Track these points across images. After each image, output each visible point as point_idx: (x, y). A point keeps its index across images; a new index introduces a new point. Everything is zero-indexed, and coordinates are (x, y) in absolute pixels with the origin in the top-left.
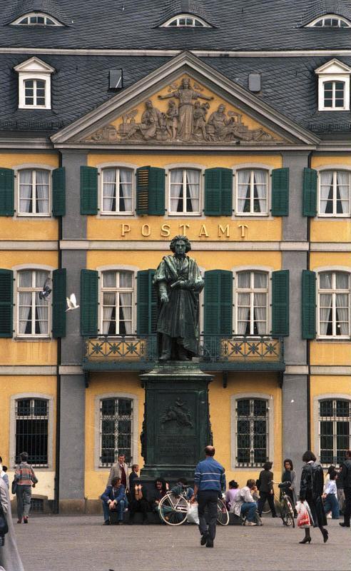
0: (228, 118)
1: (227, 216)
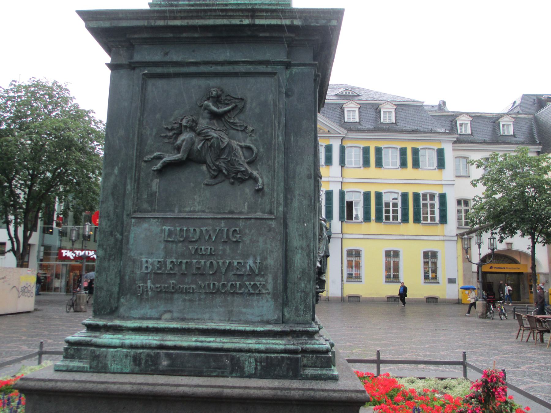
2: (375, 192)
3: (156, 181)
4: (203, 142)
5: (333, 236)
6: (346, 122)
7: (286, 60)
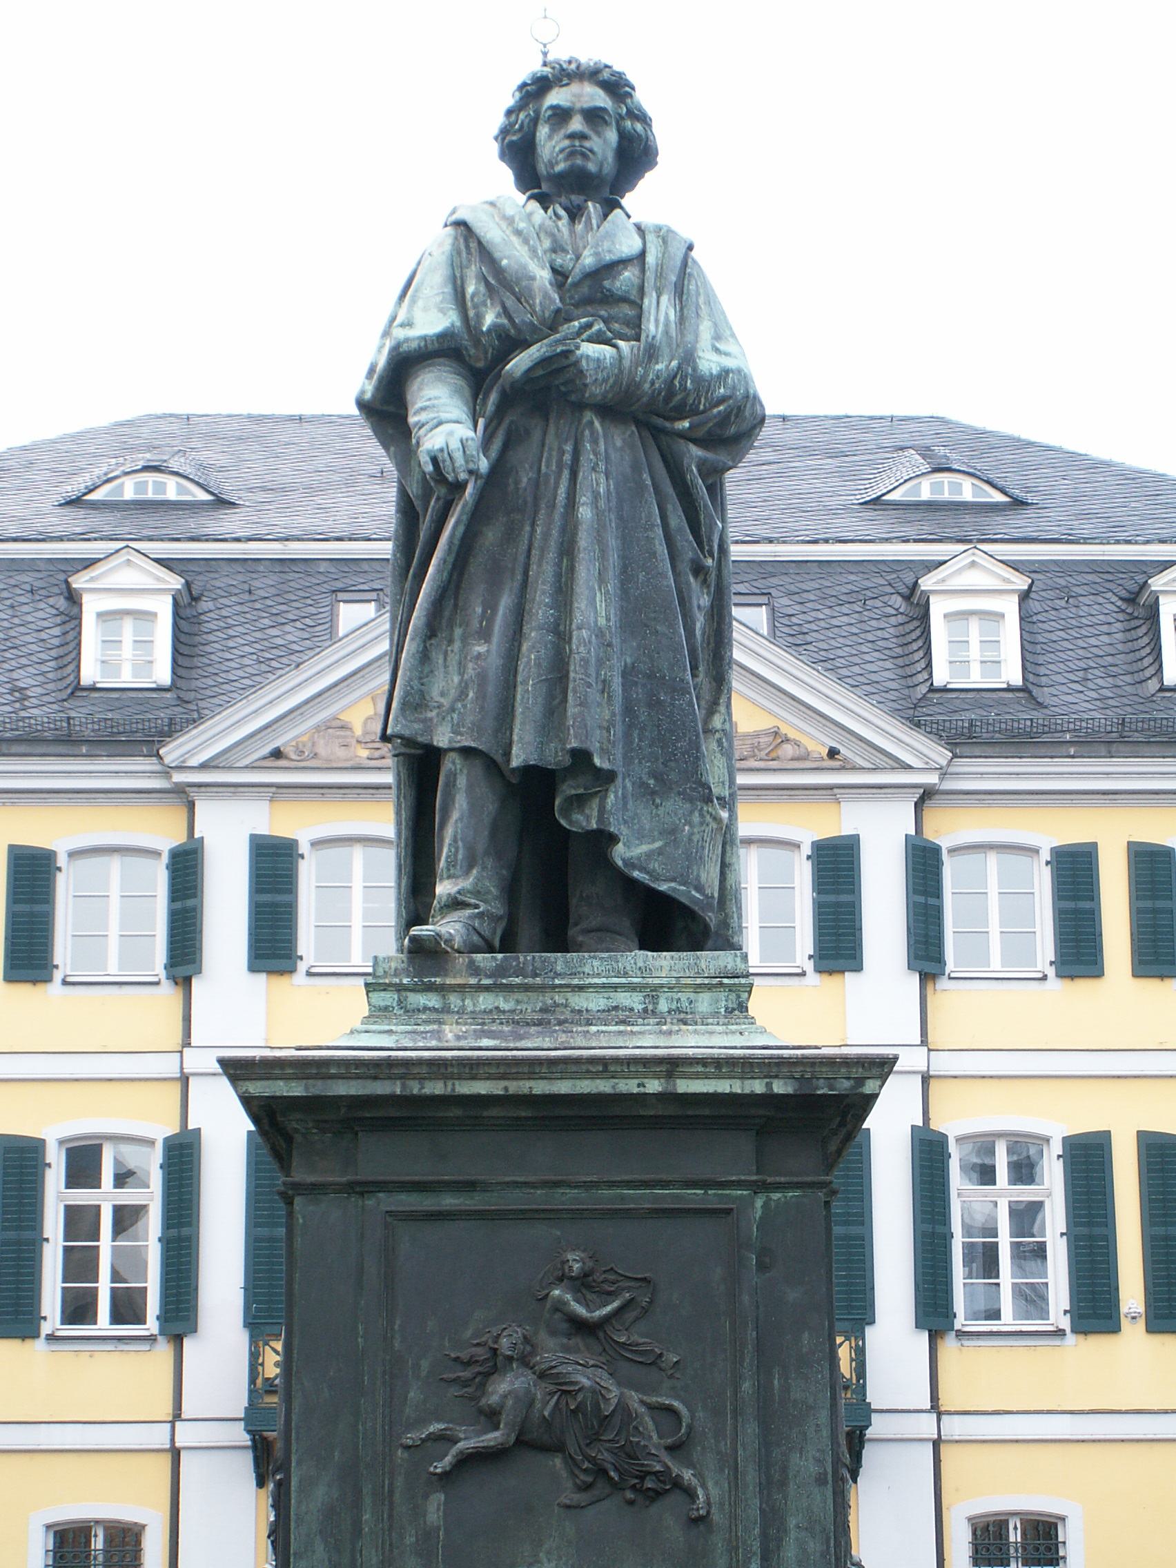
2: (1141, 1135)
3: (438, 1498)
4: (556, 1398)
5: (878, 1427)
6: (945, 690)
7: (754, 1178)
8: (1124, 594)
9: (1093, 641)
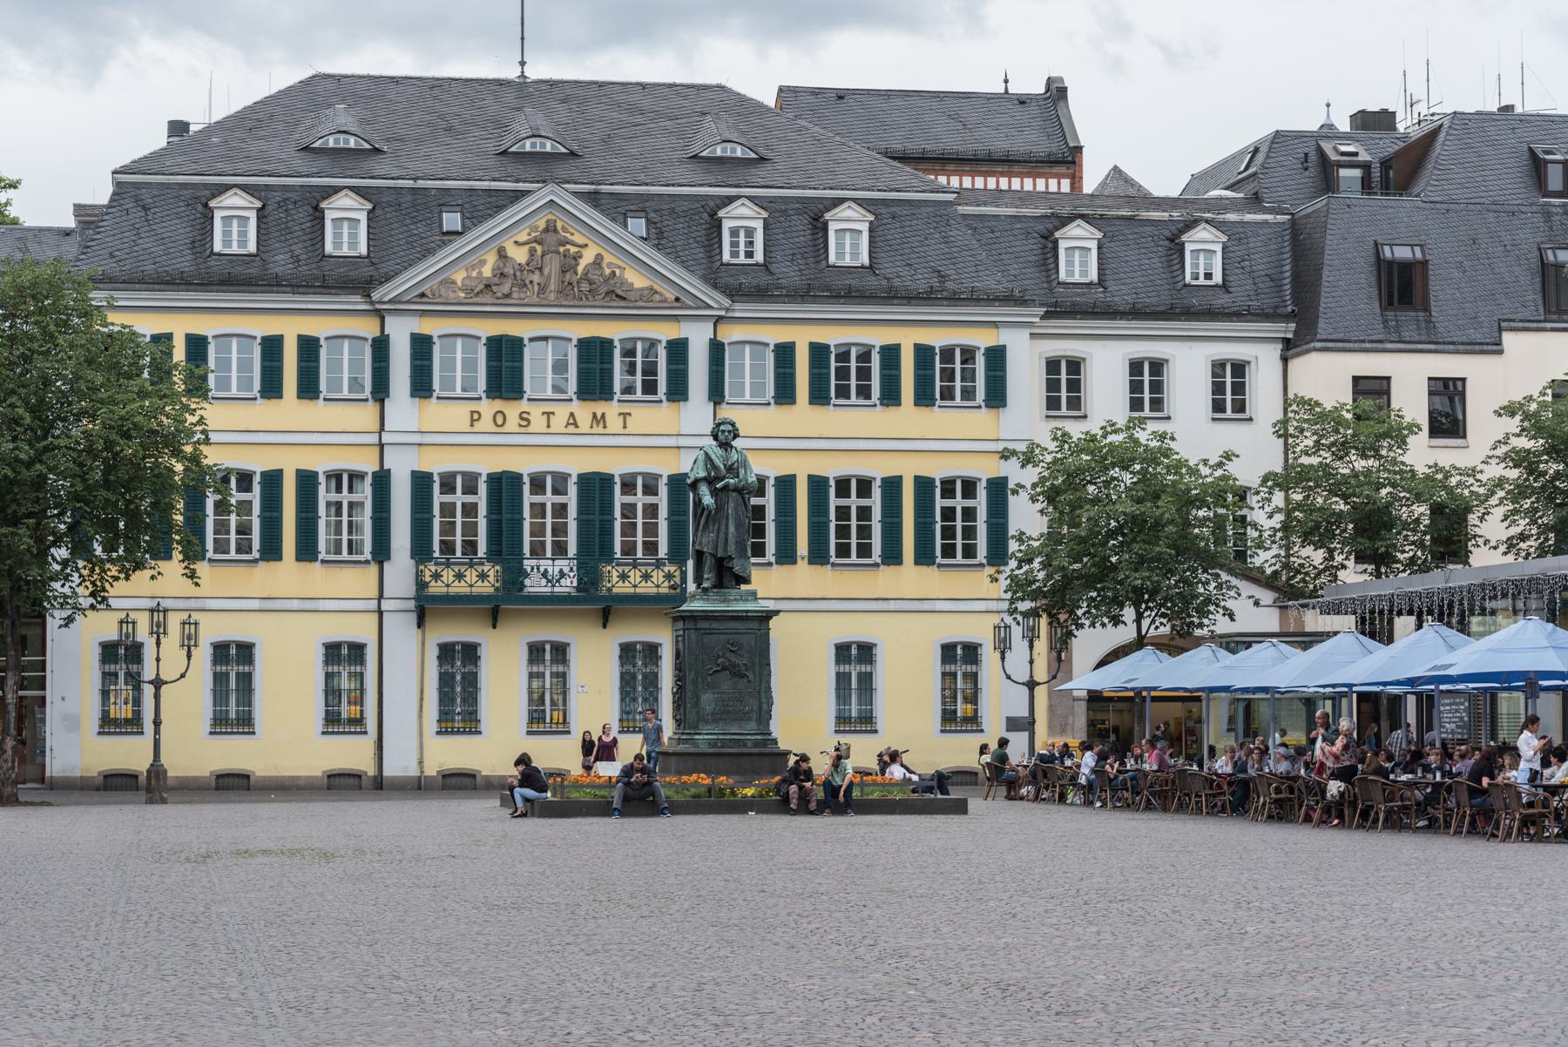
0: (607, 272)
1: (606, 400)
2: (810, 476)
6: (729, 265)
8: (812, 215)
9: (797, 240)
